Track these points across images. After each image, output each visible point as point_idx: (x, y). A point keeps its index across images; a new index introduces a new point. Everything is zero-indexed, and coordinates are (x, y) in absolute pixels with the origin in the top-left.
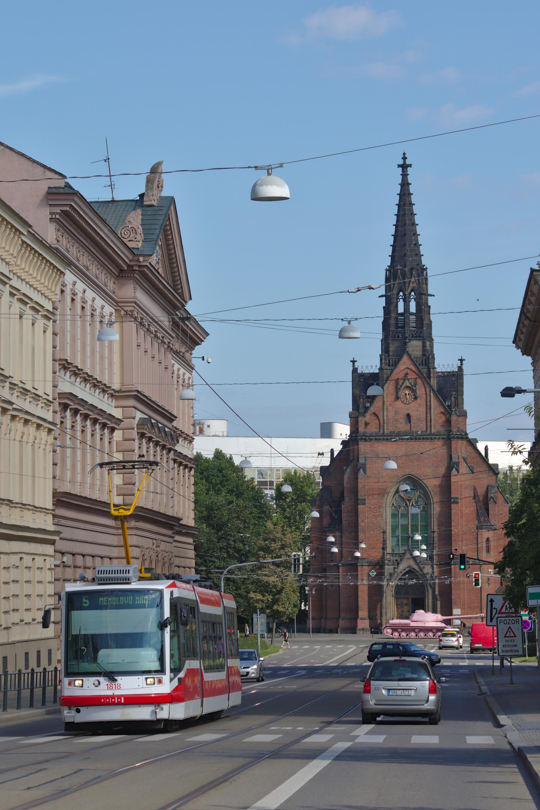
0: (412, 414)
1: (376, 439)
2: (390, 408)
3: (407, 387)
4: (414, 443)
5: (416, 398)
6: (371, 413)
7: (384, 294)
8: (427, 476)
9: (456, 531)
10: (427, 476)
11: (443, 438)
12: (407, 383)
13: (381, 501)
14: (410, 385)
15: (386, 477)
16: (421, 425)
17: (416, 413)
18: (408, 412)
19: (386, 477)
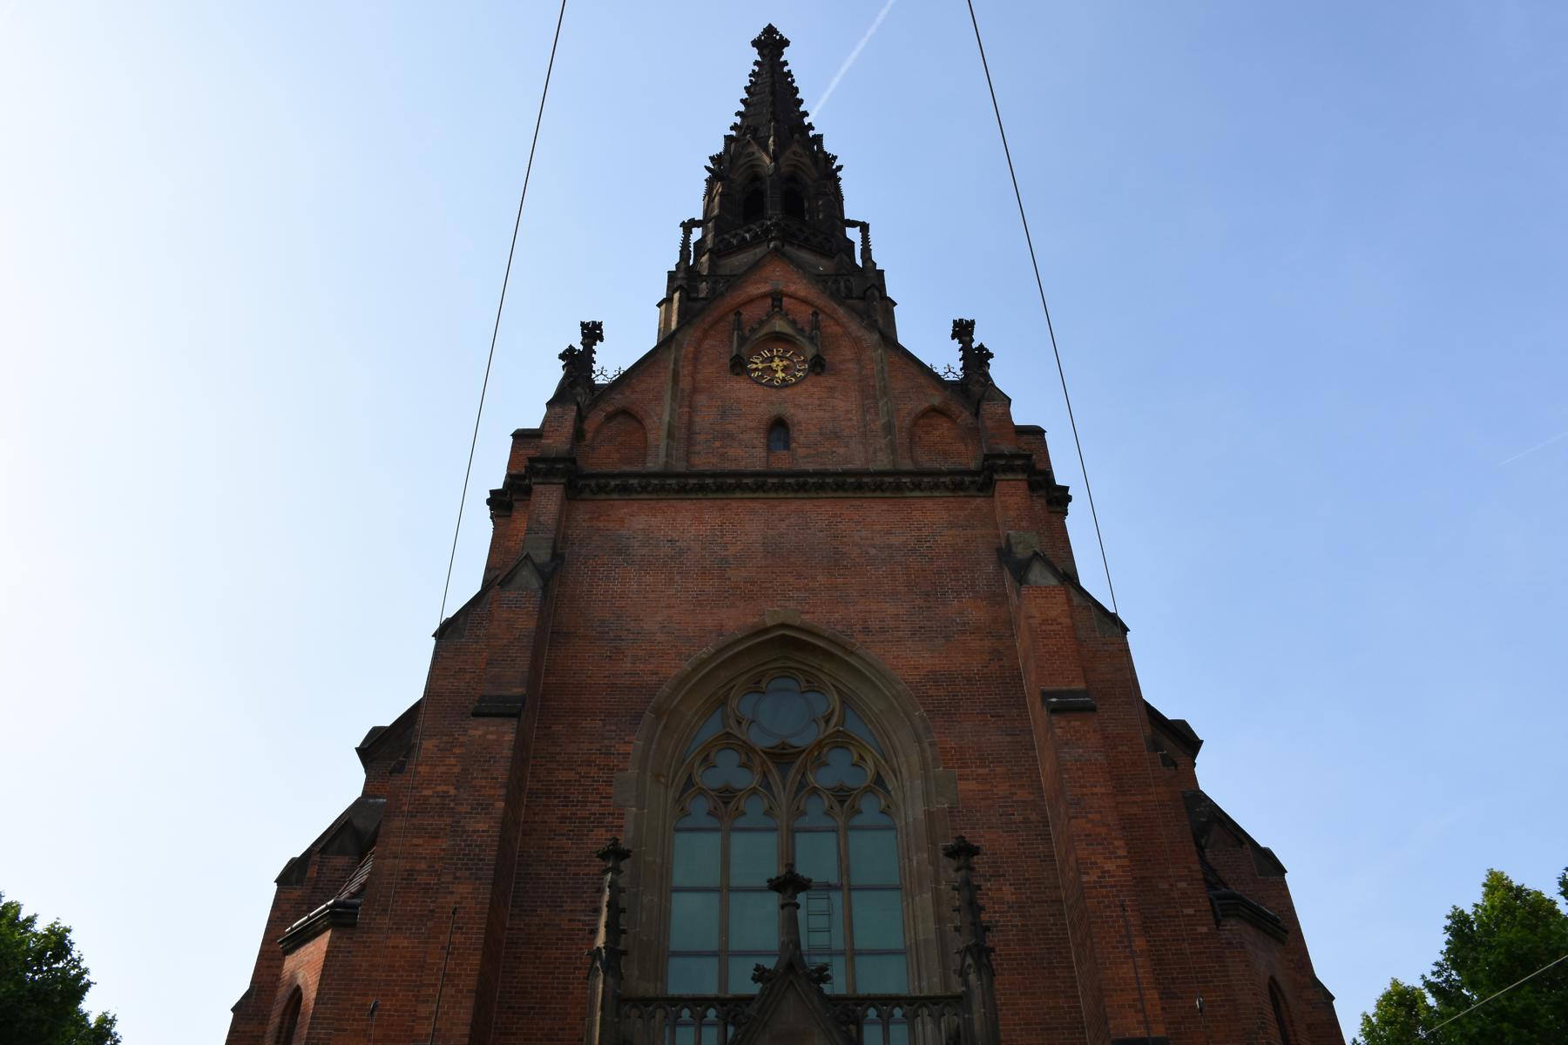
0: (796, 415)
1: (625, 489)
2: (701, 399)
3: (778, 338)
4: (808, 505)
5: (818, 366)
6: (610, 409)
7: (699, 216)
8: (883, 631)
9: (1110, 866)
10: (883, 631)
11: (957, 487)
12: (780, 325)
13: (622, 748)
14: (787, 329)
15: (660, 637)
16: (842, 450)
17: (819, 414)
18: (775, 411)
19: (660, 637)
